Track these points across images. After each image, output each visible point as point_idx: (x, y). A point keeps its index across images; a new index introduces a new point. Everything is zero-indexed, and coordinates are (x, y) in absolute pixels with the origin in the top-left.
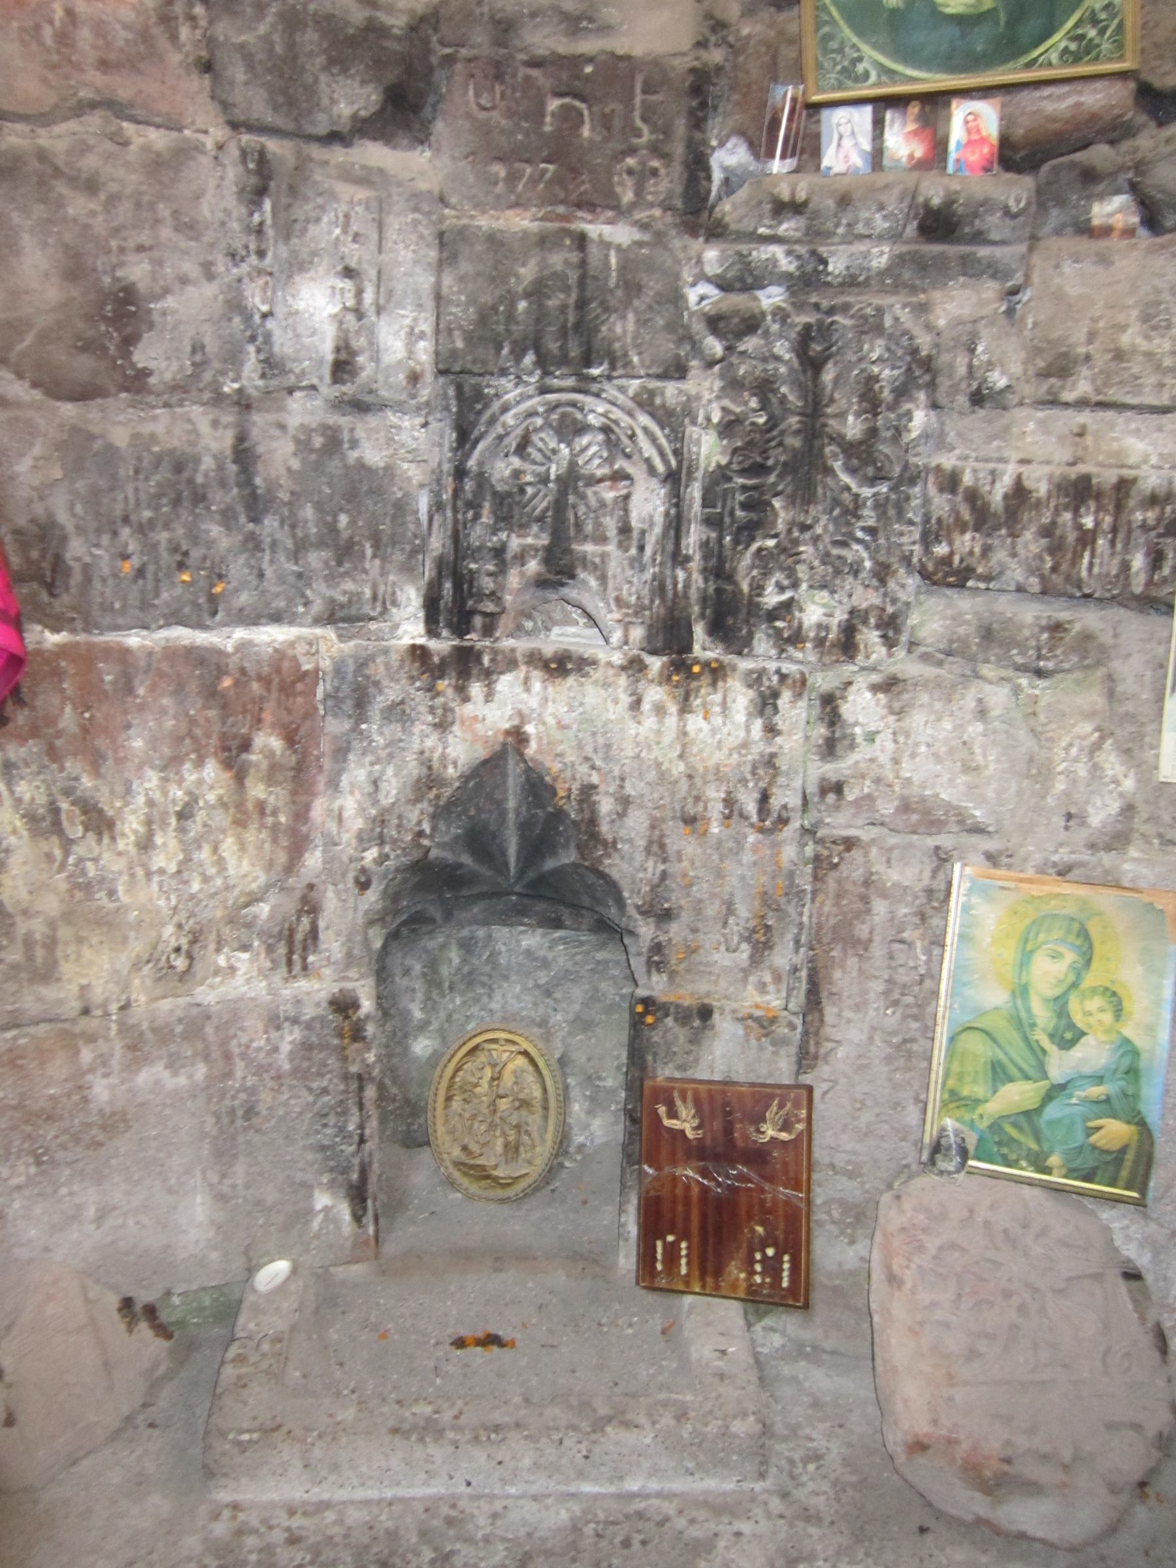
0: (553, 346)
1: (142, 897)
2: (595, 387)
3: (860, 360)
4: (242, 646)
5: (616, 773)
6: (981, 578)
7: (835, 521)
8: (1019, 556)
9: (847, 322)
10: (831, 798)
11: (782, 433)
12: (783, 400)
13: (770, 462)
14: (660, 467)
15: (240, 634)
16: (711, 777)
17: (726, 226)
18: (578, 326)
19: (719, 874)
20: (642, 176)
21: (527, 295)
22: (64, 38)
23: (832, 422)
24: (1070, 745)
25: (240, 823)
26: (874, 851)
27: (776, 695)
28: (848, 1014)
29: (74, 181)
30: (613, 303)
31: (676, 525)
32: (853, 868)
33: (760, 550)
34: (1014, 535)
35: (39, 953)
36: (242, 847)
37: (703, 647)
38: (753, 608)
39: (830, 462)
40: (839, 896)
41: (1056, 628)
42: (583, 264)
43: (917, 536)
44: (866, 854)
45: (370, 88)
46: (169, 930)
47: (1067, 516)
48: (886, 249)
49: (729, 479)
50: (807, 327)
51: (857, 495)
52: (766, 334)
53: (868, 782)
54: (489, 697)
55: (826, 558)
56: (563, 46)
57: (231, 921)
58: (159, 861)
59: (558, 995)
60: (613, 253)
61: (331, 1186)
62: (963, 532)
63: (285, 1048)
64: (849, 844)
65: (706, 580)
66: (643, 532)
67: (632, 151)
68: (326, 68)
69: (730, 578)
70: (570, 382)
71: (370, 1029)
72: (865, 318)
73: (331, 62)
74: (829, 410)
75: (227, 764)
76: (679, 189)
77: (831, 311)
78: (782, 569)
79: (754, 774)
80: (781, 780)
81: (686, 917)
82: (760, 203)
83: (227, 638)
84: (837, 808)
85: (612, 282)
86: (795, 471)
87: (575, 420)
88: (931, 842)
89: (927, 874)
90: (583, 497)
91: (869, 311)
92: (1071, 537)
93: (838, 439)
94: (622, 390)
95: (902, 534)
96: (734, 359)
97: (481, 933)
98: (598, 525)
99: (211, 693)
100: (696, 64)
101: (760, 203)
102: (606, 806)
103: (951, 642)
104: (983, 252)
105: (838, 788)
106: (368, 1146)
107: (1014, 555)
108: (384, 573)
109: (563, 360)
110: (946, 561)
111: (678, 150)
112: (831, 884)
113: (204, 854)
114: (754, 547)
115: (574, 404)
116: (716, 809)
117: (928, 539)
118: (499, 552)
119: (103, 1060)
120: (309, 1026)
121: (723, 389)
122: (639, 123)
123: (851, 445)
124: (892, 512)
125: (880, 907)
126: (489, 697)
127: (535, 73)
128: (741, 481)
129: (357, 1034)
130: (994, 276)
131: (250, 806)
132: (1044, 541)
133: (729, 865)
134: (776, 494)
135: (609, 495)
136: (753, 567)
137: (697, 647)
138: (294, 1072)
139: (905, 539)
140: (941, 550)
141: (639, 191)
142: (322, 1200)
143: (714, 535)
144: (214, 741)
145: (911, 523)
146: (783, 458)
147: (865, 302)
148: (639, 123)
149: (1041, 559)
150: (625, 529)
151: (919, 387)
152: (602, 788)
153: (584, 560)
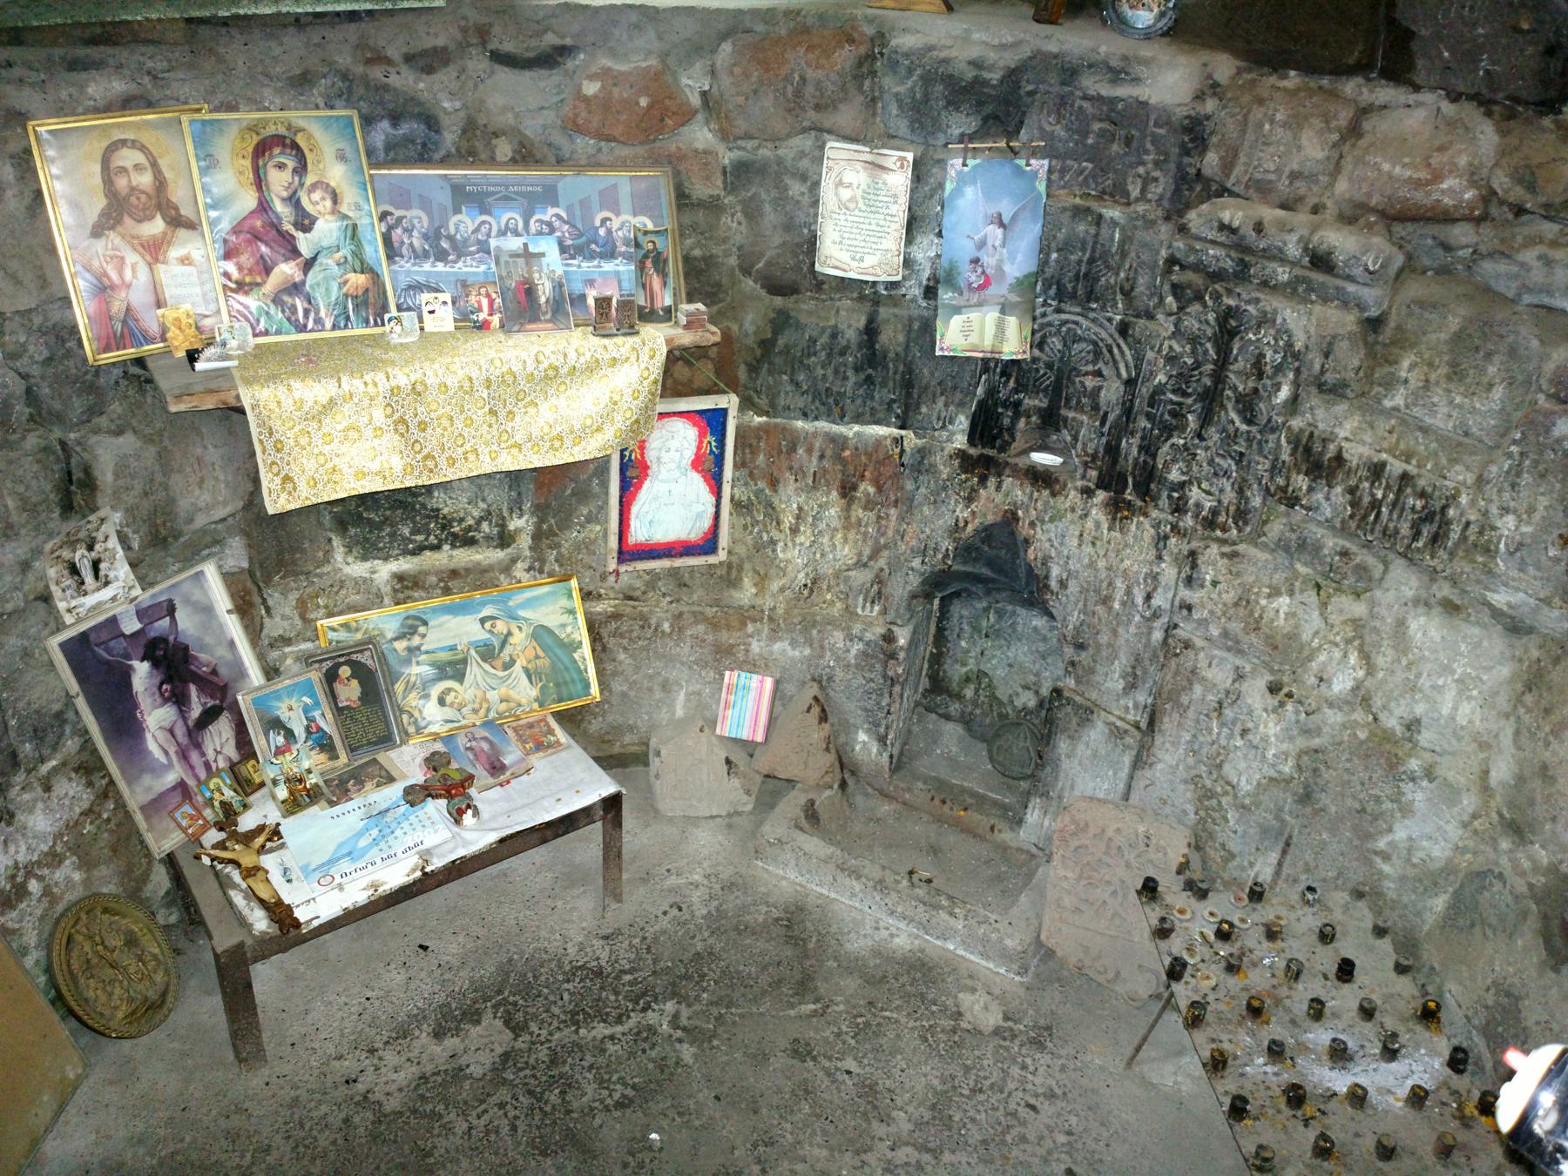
0: (1069, 286)
1: (789, 555)
2: (1092, 315)
4: (857, 434)
5: (1065, 552)
8: (1331, 501)
10: (1185, 612)
12: (1206, 352)
15: (857, 428)
18: (1086, 275)
19: (1115, 633)
20: (1147, 181)
21: (1058, 250)
22: (798, 94)
25: (847, 528)
26: (1202, 655)
27: (1166, 537)
28: (1167, 745)
29: (794, 175)
30: (1112, 262)
31: (1128, 412)
32: (1188, 659)
34: (1330, 486)
35: (734, 573)
36: (846, 540)
37: (1129, 495)
38: (1162, 480)
40: (1177, 673)
41: (1345, 554)
42: (1097, 235)
45: (971, 118)
46: (801, 575)
47: (1366, 485)
50: (1229, 308)
52: (1205, 306)
54: (998, 488)
55: (1211, 462)
56: (1106, 91)
57: (837, 575)
58: (800, 539)
59: (1049, 660)
61: (868, 731)
63: (854, 652)
64: (1187, 645)
66: (1106, 414)
67: (1143, 163)
68: (946, 107)
70: (1078, 309)
71: (902, 655)
73: (949, 103)
75: (844, 495)
76: (1169, 194)
77: (1248, 302)
80: (1160, 590)
81: (1091, 651)
83: (851, 430)
84: (1186, 619)
85: (1114, 250)
87: (1075, 334)
88: (1239, 662)
89: (1229, 681)
90: (1074, 383)
91: (1268, 309)
92: (1366, 500)
93: (1235, 388)
97: (1009, 608)
98: (1079, 402)
99: (838, 458)
100: (1193, 113)
102: (1055, 571)
104: (1351, 288)
105: (1189, 608)
106: (890, 718)
107: (1328, 499)
108: (946, 405)
109: (1073, 296)
110: (1284, 490)
111: (1172, 166)
112: (1173, 663)
113: (825, 540)
114: (1174, 440)
115: (1076, 323)
116: (1119, 594)
117: (1274, 470)
118: (1018, 403)
119: (759, 632)
120: (868, 644)
122: (1149, 146)
124: (1255, 446)
125: (1198, 689)
126: (998, 488)
127: (1086, 104)
128: (1171, 396)
129: (892, 656)
131: (853, 520)
132: (1348, 497)
133: (1121, 630)
135: (1090, 383)
138: (857, 666)
140: (1281, 481)
141: (1143, 191)
142: (862, 736)
144: (838, 483)
147: (1271, 302)
148: (1149, 146)
153: (1066, 419)
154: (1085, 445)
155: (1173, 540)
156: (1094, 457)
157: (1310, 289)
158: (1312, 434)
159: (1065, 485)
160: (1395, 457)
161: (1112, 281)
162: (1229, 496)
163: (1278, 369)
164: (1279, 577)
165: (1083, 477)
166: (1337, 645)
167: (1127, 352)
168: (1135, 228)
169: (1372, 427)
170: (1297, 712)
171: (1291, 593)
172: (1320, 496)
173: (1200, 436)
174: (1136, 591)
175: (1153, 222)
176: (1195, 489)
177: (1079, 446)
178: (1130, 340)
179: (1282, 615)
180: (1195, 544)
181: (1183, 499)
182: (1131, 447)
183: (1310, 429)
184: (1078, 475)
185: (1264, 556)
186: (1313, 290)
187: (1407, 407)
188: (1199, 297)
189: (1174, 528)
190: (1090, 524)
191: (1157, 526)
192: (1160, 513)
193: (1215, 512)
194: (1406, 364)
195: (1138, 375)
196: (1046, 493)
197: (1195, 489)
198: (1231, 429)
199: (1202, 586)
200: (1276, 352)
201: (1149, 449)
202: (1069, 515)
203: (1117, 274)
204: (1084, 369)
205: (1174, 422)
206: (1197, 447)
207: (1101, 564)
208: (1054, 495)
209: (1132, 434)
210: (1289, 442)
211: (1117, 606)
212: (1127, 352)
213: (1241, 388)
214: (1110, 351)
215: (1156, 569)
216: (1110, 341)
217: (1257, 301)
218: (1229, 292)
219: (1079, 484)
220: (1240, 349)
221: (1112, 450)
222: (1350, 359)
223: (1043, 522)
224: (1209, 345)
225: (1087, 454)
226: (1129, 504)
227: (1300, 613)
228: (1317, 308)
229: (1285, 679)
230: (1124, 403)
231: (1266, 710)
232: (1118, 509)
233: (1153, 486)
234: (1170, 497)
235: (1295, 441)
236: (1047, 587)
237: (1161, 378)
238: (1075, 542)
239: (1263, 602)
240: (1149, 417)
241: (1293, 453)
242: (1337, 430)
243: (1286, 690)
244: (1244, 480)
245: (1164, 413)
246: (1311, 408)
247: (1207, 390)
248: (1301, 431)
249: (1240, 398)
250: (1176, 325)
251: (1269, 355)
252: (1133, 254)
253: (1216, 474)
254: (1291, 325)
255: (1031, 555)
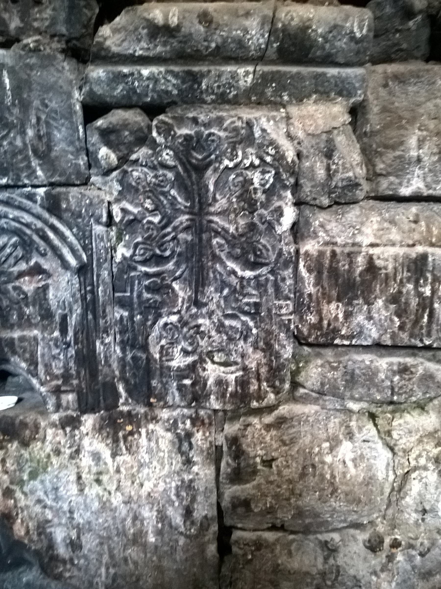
3: (236, 166)
5: (66, 507)
6: (342, 337)
7: (226, 298)
8: (374, 319)
9: (222, 134)
10: (241, 510)
11: (175, 229)
12: (173, 202)
13: (168, 253)
14: (73, 262)
16: (144, 501)
17: (108, 49)
23: (216, 219)
24: (420, 456)
27: (189, 435)
31: (91, 305)
33: (166, 324)
34: (369, 303)
38: (165, 371)
39: (217, 251)
41: (404, 370)
43: (291, 308)
44: (272, 551)
47: (410, 286)
48: (251, 69)
49: (135, 269)
50: (188, 138)
51: (242, 278)
52: (154, 145)
53: (269, 499)
55: (220, 328)
60: (5, 73)
62: (329, 302)
65: (123, 350)
66: (64, 318)
69: (145, 348)
72: (236, 130)
74: (212, 209)
76: (62, 16)
77: (208, 125)
78: (185, 338)
79: (178, 495)
80: (199, 498)
82: (136, 29)
85: (8, 100)
86: (188, 260)
89: (320, 560)
91: (239, 124)
92: (414, 302)
93: (222, 233)
94: (31, 197)
95: (281, 307)
96: (125, 167)
101: (136, 29)
102: (59, 535)
103: (322, 384)
104: (332, 71)
107: (370, 318)
110: (318, 326)
121: (120, 193)
123: (233, 236)
128: (144, 269)
130: (340, 94)
134: (175, 279)
135: (29, 286)
136: (161, 337)
137: (121, 401)
139: (284, 311)
140: (312, 318)
143: (126, 314)
145: (288, 298)
146: (178, 250)
149: (392, 320)
150: (47, 315)
151: (285, 187)
152: (56, 520)
154: (47, 366)
155: (199, 436)
156: (66, 377)
157: (282, 88)
158: (334, 253)
159: (37, 427)
160: (432, 245)
161: (19, 143)
162: (255, 359)
163: (270, 192)
164: (334, 423)
165: (58, 407)
166: (425, 468)
167: (68, 233)
168: (31, 67)
169: (392, 222)
170: (410, 559)
171: (350, 436)
172: (360, 318)
173: (198, 304)
174: (170, 511)
175: (51, 58)
176: (209, 366)
177: (41, 369)
178: (67, 215)
179: (350, 464)
180: (231, 429)
181: (200, 382)
182: (110, 349)
183: (328, 250)
184: (50, 406)
185: (310, 409)
186: (284, 88)
187: (428, 187)
188: (143, 139)
189: (196, 421)
190: (86, 461)
191: (172, 427)
192: (174, 410)
193: (242, 383)
194: (413, 141)
195: (90, 257)
196: (13, 446)
197: (209, 366)
198: (234, 281)
199: (255, 472)
200: (263, 172)
201: (134, 339)
202: (54, 460)
203: (23, 133)
204: (15, 270)
205: (158, 298)
206: (195, 317)
207: (117, 500)
208: (25, 444)
209: (106, 331)
210: (310, 271)
211: (152, 539)
212: (68, 233)
213: (232, 229)
214: (45, 238)
215: (187, 477)
216: (39, 224)
217: (220, 121)
218: (180, 121)
219: (55, 417)
220: (216, 184)
221: (87, 359)
222: (350, 158)
223: (21, 483)
224: (173, 192)
225: (57, 377)
226: (130, 417)
227: (367, 452)
228: (294, 110)
229: (381, 529)
230: (84, 298)
231: (375, 573)
232: (117, 428)
233: (154, 383)
234: (181, 388)
235: (316, 266)
236: (55, 559)
237: (122, 252)
238: (74, 489)
239: (328, 459)
240: (123, 303)
241: (318, 282)
242: (359, 239)
243: (387, 541)
244: (269, 333)
245: (139, 291)
246: (322, 226)
247: (190, 246)
248: (321, 254)
249: (232, 241)
250: (121, 182)
251: (256, 178)
252: (36, 103)
253: (231, 339)
254: (274, 136)
255: (19, 530)
